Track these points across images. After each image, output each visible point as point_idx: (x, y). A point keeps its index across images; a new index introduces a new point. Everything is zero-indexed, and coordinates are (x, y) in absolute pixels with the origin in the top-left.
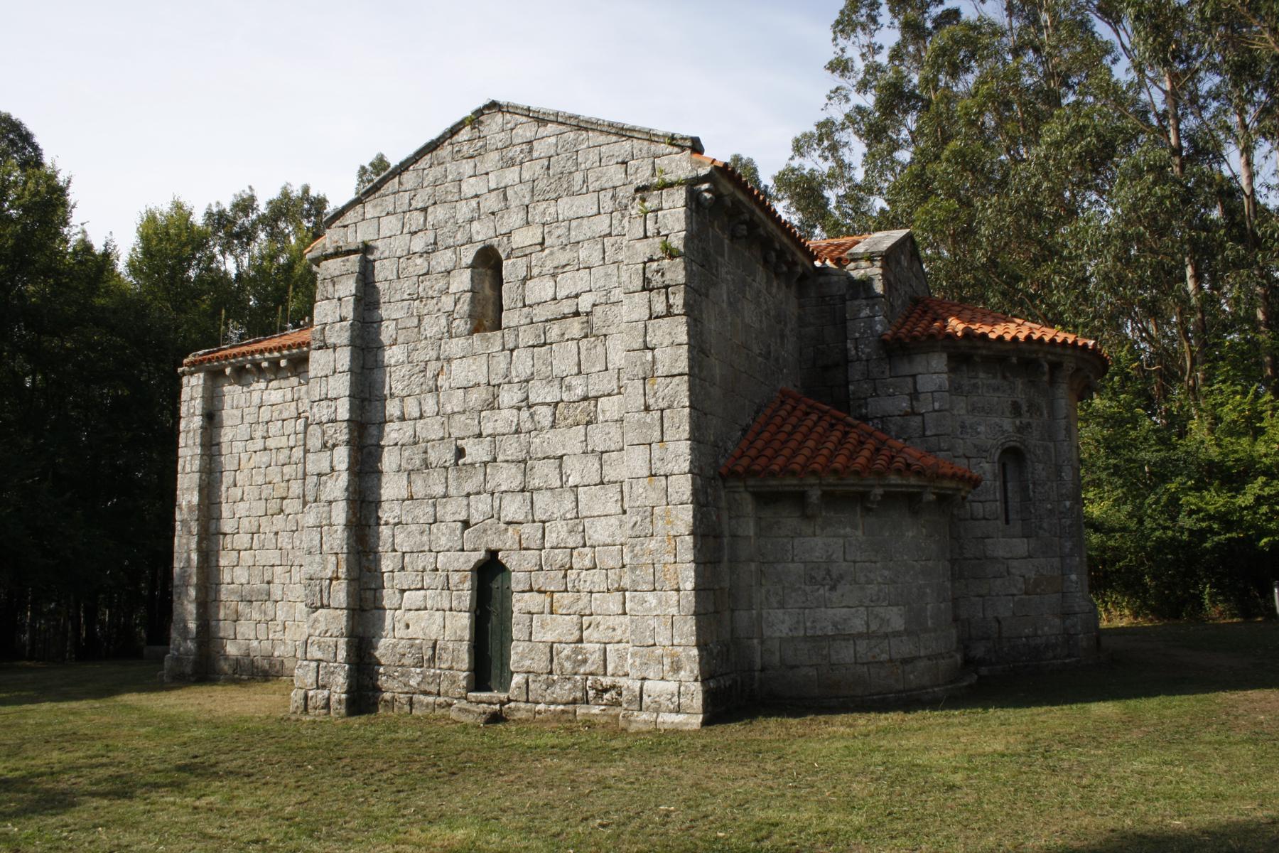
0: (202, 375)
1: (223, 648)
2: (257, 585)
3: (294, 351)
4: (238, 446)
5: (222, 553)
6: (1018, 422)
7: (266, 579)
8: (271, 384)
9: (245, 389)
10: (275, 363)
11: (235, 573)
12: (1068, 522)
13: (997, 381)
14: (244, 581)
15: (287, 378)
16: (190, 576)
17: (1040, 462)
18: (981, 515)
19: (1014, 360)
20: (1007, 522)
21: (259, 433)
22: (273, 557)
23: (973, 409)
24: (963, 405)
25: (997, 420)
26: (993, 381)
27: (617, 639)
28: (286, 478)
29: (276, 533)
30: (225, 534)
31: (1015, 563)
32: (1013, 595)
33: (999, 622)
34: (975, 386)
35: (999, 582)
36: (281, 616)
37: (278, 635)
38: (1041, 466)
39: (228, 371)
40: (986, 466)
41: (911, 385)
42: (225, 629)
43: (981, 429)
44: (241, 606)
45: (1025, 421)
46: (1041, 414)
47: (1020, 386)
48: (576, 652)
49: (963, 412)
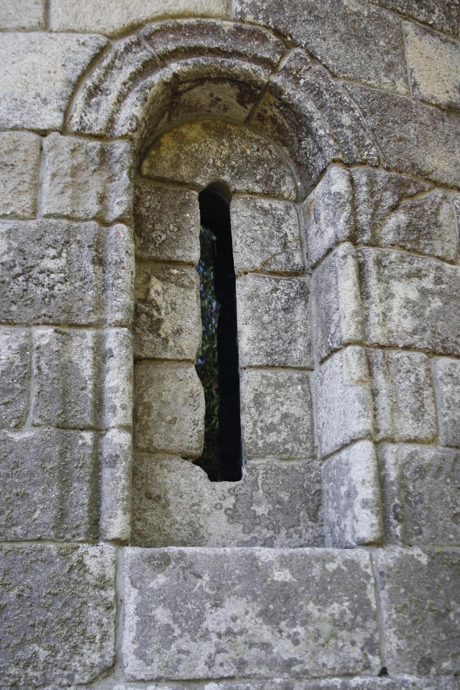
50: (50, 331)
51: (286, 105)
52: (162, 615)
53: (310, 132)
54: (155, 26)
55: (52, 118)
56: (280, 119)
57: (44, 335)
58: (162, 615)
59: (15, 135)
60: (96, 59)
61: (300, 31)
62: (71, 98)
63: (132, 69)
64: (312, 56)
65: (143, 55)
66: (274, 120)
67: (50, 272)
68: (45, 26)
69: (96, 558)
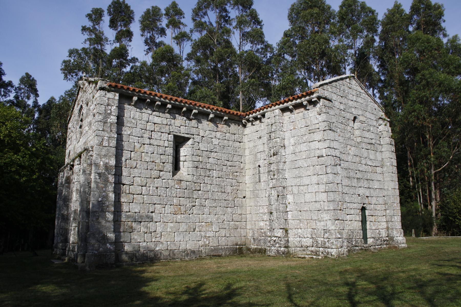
0: (117, 95)
1: (123, 247)
2: (144, 212)
3: (177, 103)
4: (133, 139)
5: (122, 195)
7: (151, 210)
8: (154, 113)
9: (138, 110)
10: (164, 105)
11: (130, 207)
14: (137, 211)
15: (164, 113)
16: (108, 206)
21: (147, 135)
22: (155, 199)
28: (164, 161)
29: (157, 188)
30: (124, 185)
36: (159, 229)
37: (157, 239)
39: (135, 98)
42: (124, 237)
44: (134, 225)
48: (379, 231)
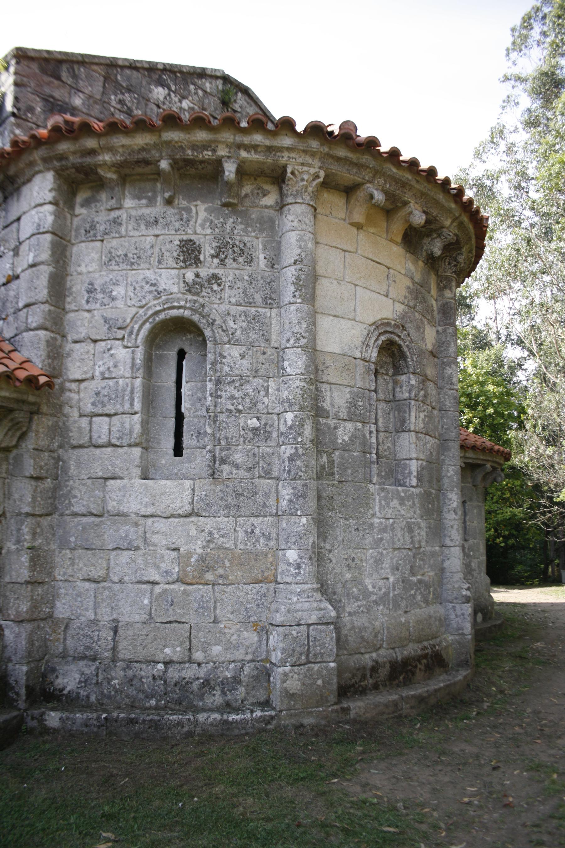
6: (190, 275)
12: (287, 451)
13: (159, 209)
17: (237, 343)
18: (104, 439)
19: (164, 165)
20: (178, 451)
23: (110, 259)
24: (95, 255)
25: (149, 274)
26: (146, 211)
27: (97, 595)
31: (161, 525)
32: (154, 583)
33: (115, 631)
34: (116, 222)
35: (125, 557)
38: (236, 351)
40: (121, 353)
41: (15, 235)
43: (118, 291)
45: (204, 272)
46: (249, 261)
47: (203, 214)
49: (94, 266)
50: (360, 424)
51: (401, 350)
52: (383, 502)
53: (405, 360)
54: (379, 323)
55: (358, 355)
56: (396, 352)
57: (359, 425)
58: (383, 502)
59: (351, 358)
60: (368, 335)
61: (407, 325)
62: (362, 348)
63: (374, 339)
64: (409, 335)
65: (376, 333)
66: (393, 351)
67: (360, 406)
68: (354, 320)
69: (371, 487)
